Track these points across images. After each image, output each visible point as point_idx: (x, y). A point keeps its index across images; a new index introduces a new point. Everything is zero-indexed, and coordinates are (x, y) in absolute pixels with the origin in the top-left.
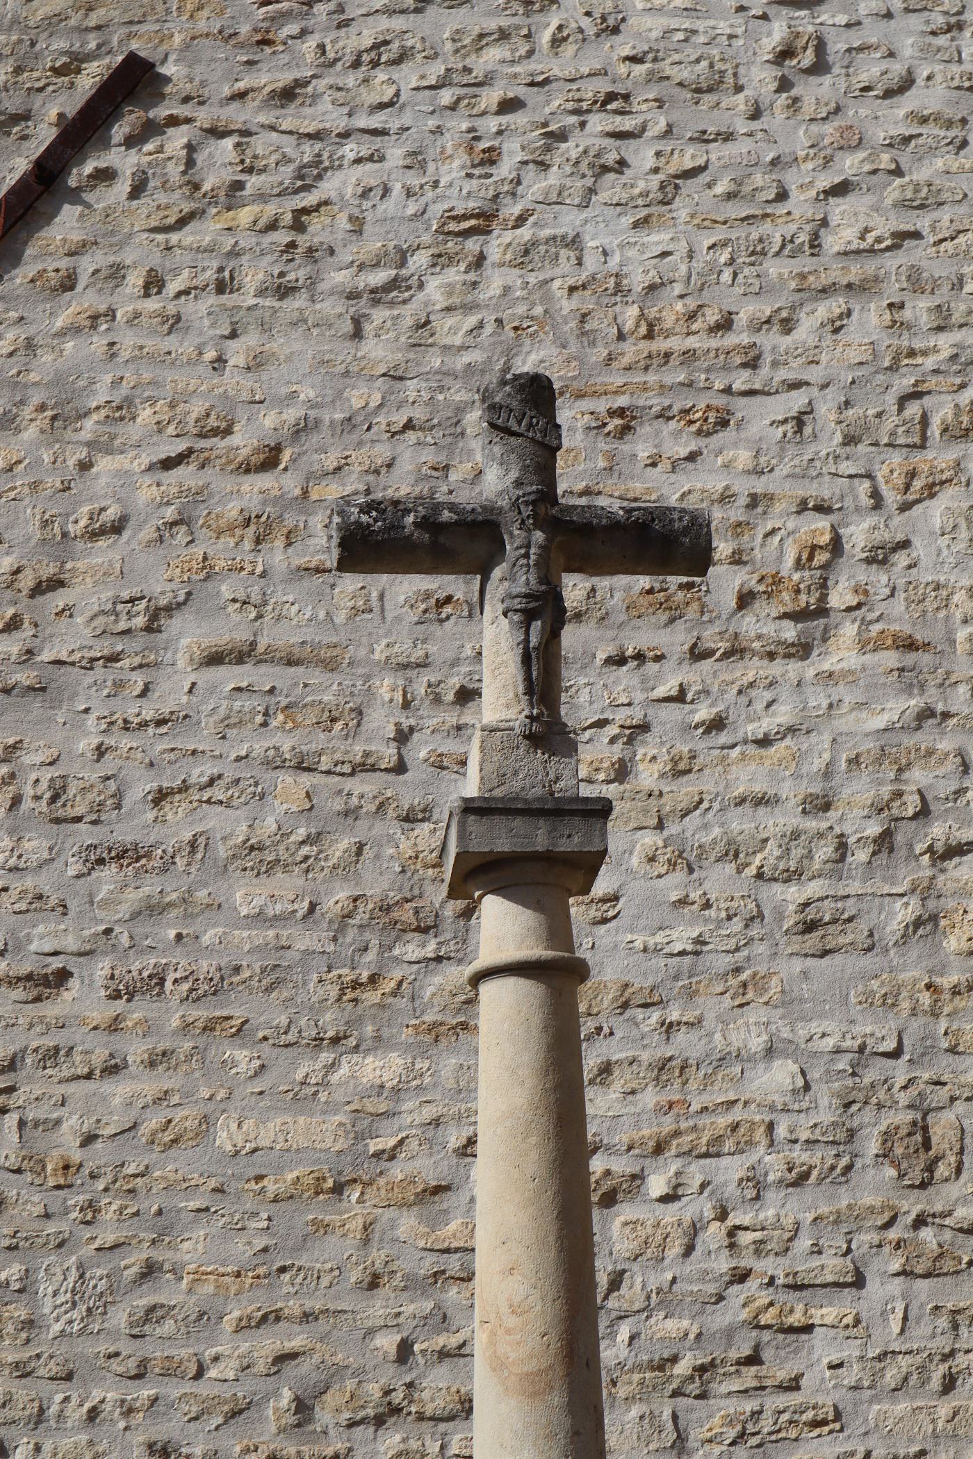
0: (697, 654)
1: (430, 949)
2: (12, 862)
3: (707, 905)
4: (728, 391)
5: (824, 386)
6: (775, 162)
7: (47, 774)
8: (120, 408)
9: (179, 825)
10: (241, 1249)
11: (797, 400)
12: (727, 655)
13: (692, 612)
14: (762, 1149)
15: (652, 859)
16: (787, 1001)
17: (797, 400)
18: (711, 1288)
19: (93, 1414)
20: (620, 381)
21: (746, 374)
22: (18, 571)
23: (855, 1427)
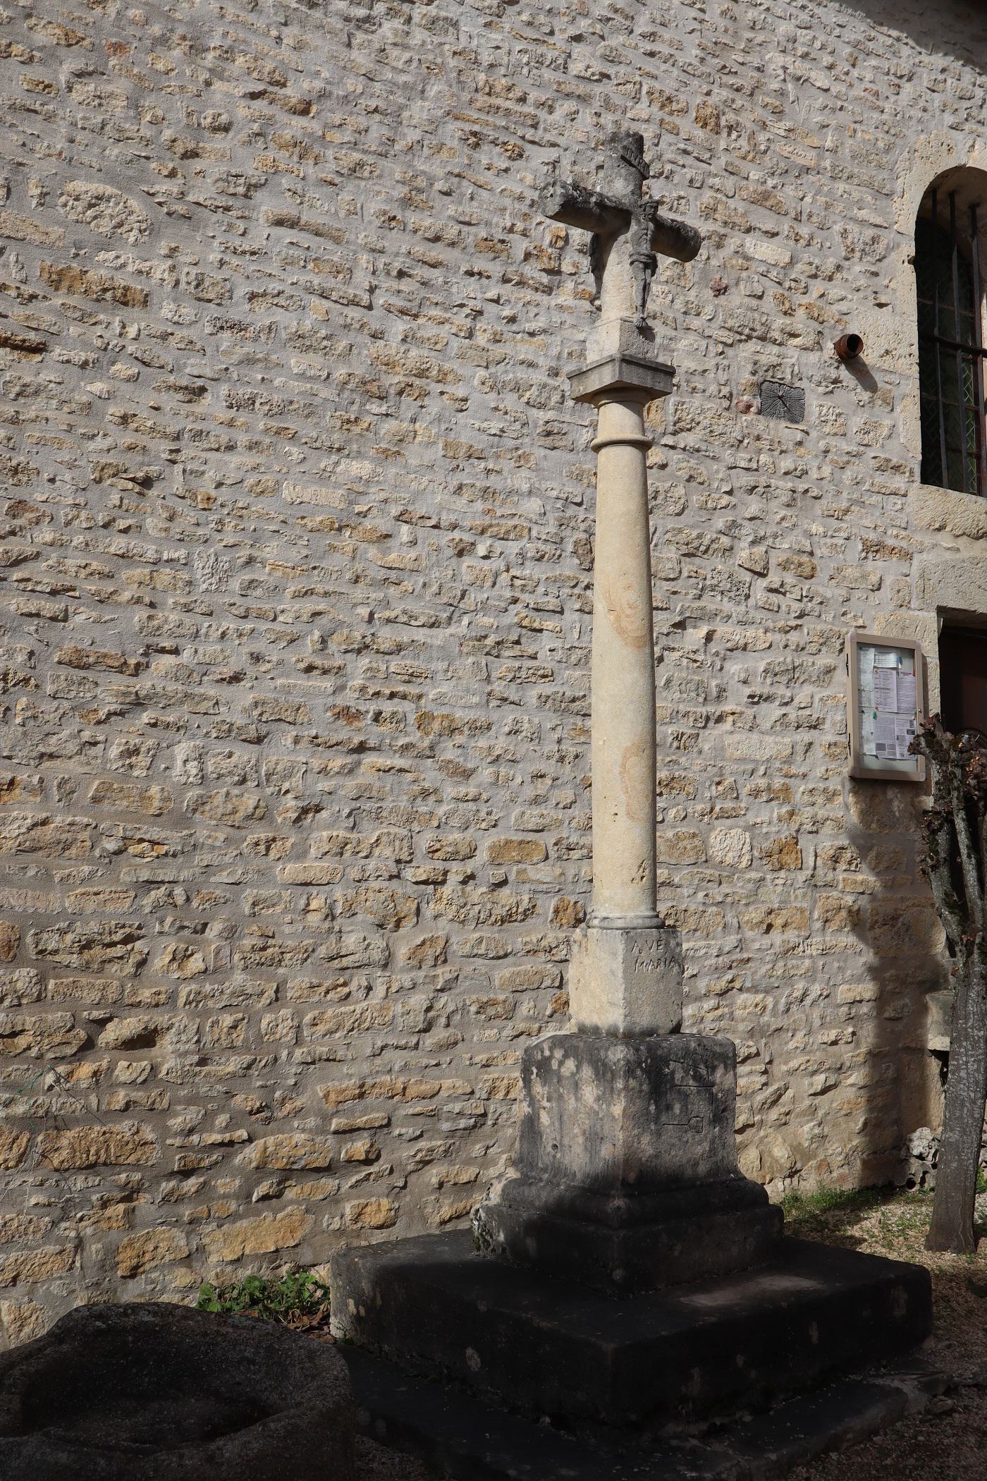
0: (505, 280)
1: (383, 409)
2: (176, 318)
3: (506, 413)
4: (523, 138)
5: (566, 150)
6: (550, 11)
7: (194, 271)
8: (227, 52)
9: (262, 316)
10: (295, 555)
11: (553, 154)
12: (518, 284)
13: (504, 256)
14: (525, 540)
15: (483, 384)
16: (537, 469)
17: (553, 154)
18: (503, 605)
19: (223, 635)
20: (476, 116)
21: (533, 131)
22: (174, 141)
23: (559, 680)
